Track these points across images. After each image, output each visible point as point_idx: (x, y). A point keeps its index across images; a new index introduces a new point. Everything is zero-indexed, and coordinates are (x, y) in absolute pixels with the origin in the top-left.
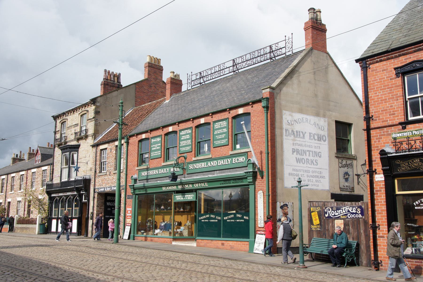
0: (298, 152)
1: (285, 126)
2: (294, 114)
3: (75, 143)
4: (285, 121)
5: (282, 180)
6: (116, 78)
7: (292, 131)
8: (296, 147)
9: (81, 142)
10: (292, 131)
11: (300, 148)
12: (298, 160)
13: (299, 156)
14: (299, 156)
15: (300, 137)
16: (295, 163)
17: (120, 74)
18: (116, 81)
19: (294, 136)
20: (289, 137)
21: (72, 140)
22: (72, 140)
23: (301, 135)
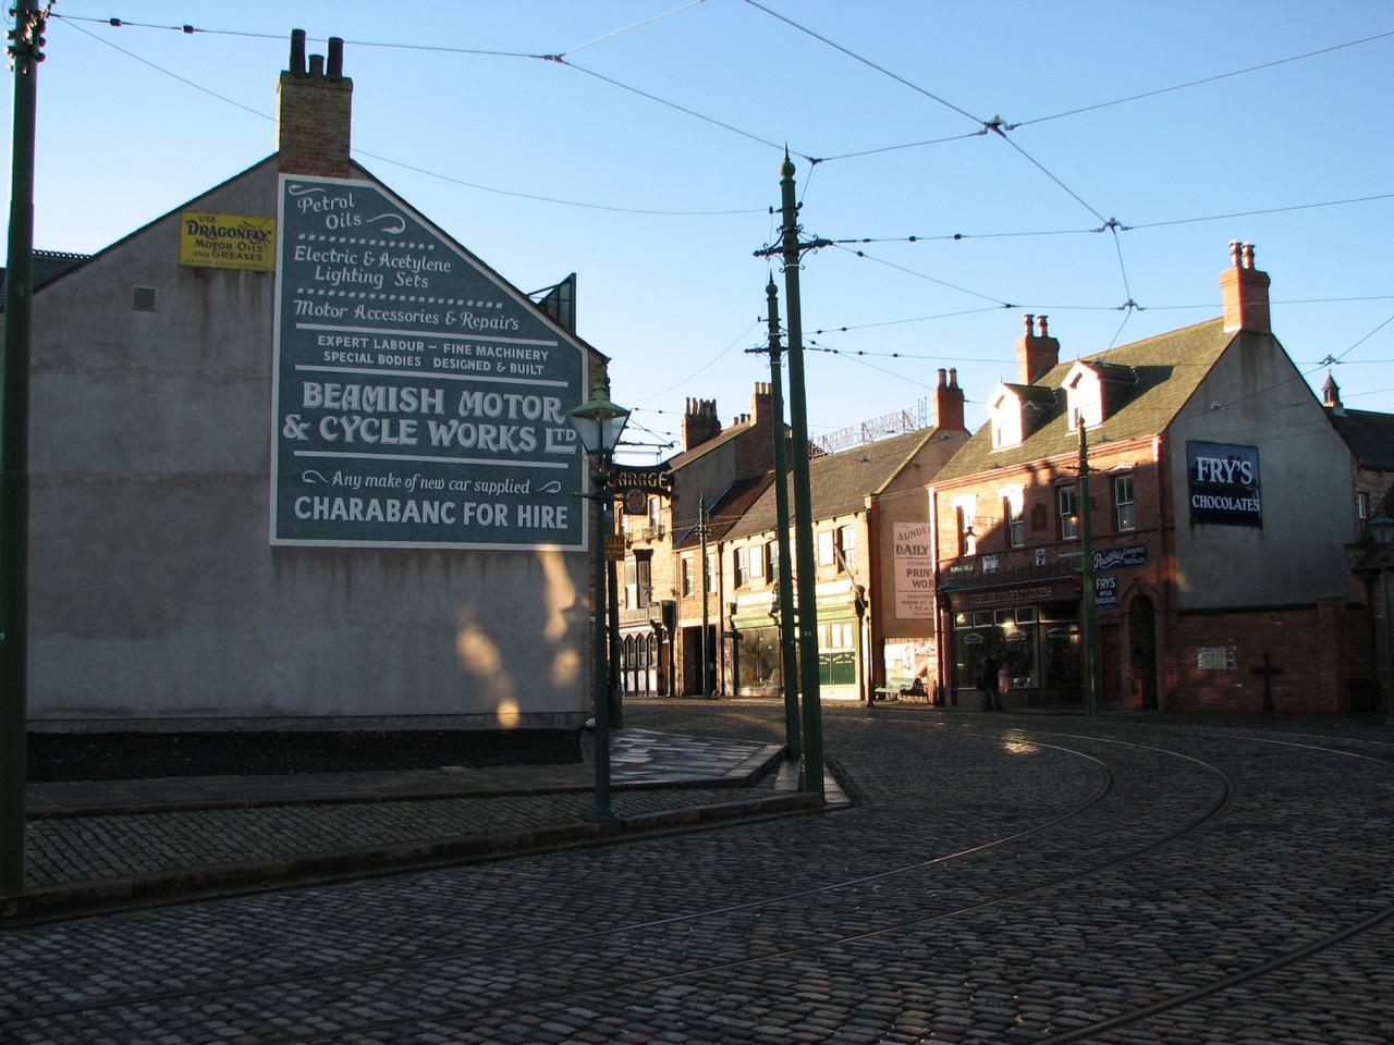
0: (916, 572)
1: (897, 541)
2: (909, 524)
3: (644, 546)
4: (896, 536)
5: (893, 610)
6: (708, 409)
7: (907, 546)
8: (912, 568)
9: (655, 545)
10: (907, 546)
11: (919, 568)
12: (916, 584)
13: (916, 579)
14: (916, 579)
15: (919, 553)
16: (913, 588)
17: (714, 401)
18: (709, 415)
19: (910, 553)
20: (902, 556)
21: (639, 541)
22: (639, 541)
23: (922, 550)
